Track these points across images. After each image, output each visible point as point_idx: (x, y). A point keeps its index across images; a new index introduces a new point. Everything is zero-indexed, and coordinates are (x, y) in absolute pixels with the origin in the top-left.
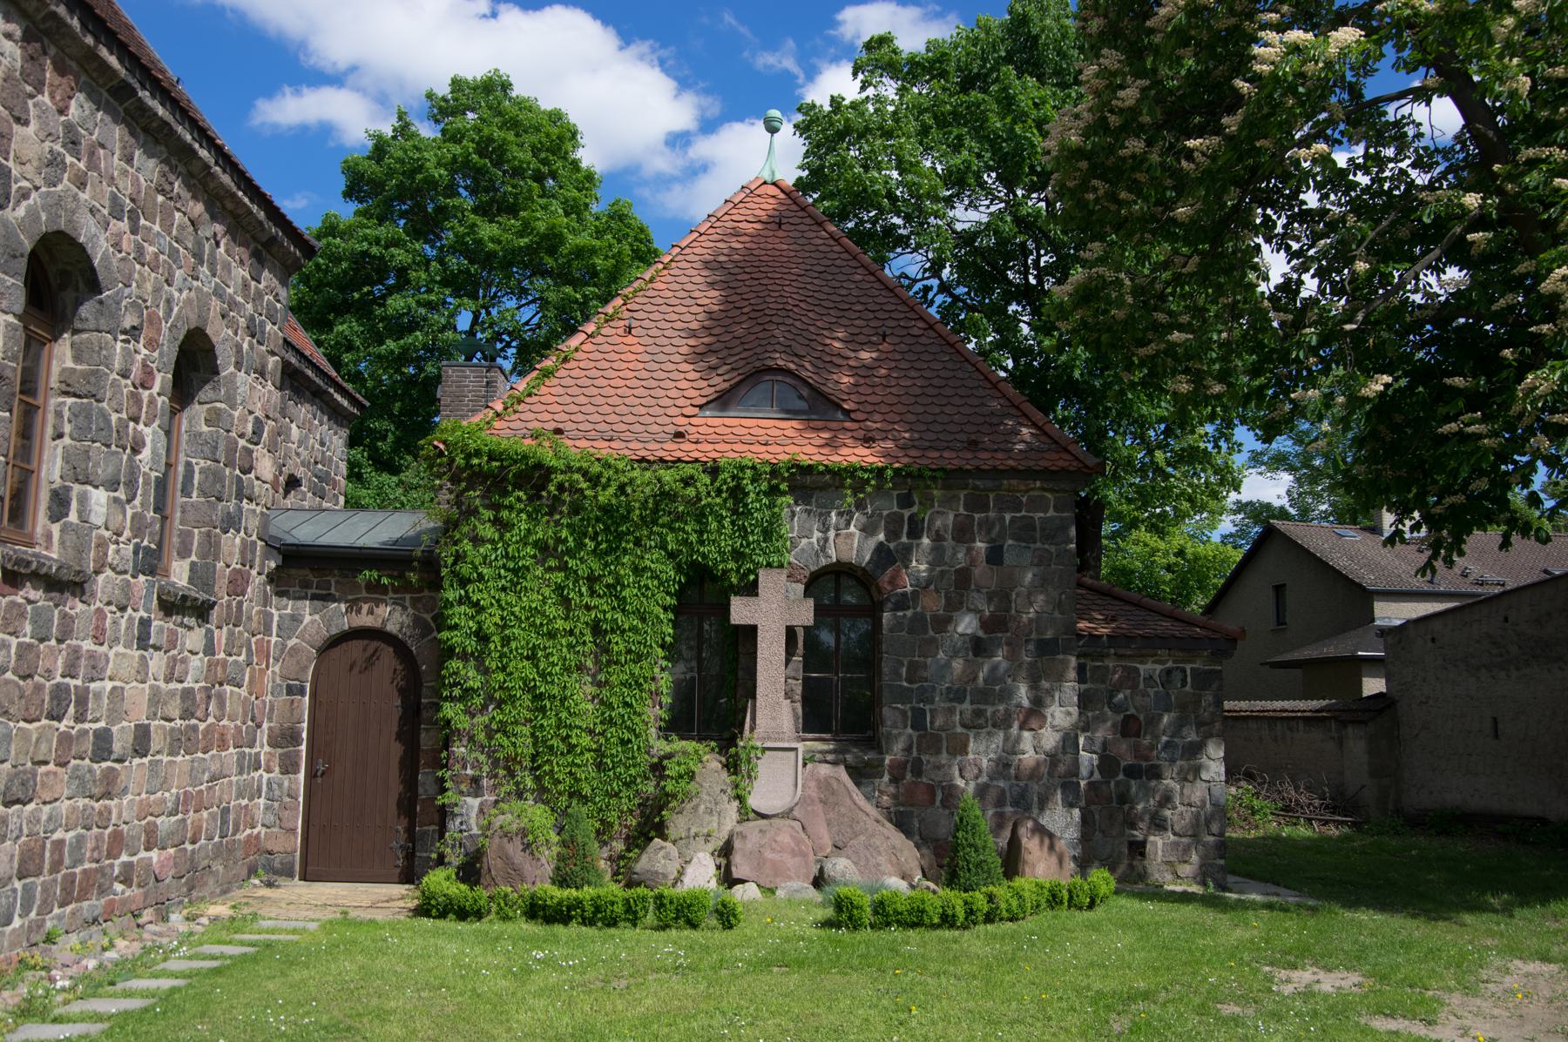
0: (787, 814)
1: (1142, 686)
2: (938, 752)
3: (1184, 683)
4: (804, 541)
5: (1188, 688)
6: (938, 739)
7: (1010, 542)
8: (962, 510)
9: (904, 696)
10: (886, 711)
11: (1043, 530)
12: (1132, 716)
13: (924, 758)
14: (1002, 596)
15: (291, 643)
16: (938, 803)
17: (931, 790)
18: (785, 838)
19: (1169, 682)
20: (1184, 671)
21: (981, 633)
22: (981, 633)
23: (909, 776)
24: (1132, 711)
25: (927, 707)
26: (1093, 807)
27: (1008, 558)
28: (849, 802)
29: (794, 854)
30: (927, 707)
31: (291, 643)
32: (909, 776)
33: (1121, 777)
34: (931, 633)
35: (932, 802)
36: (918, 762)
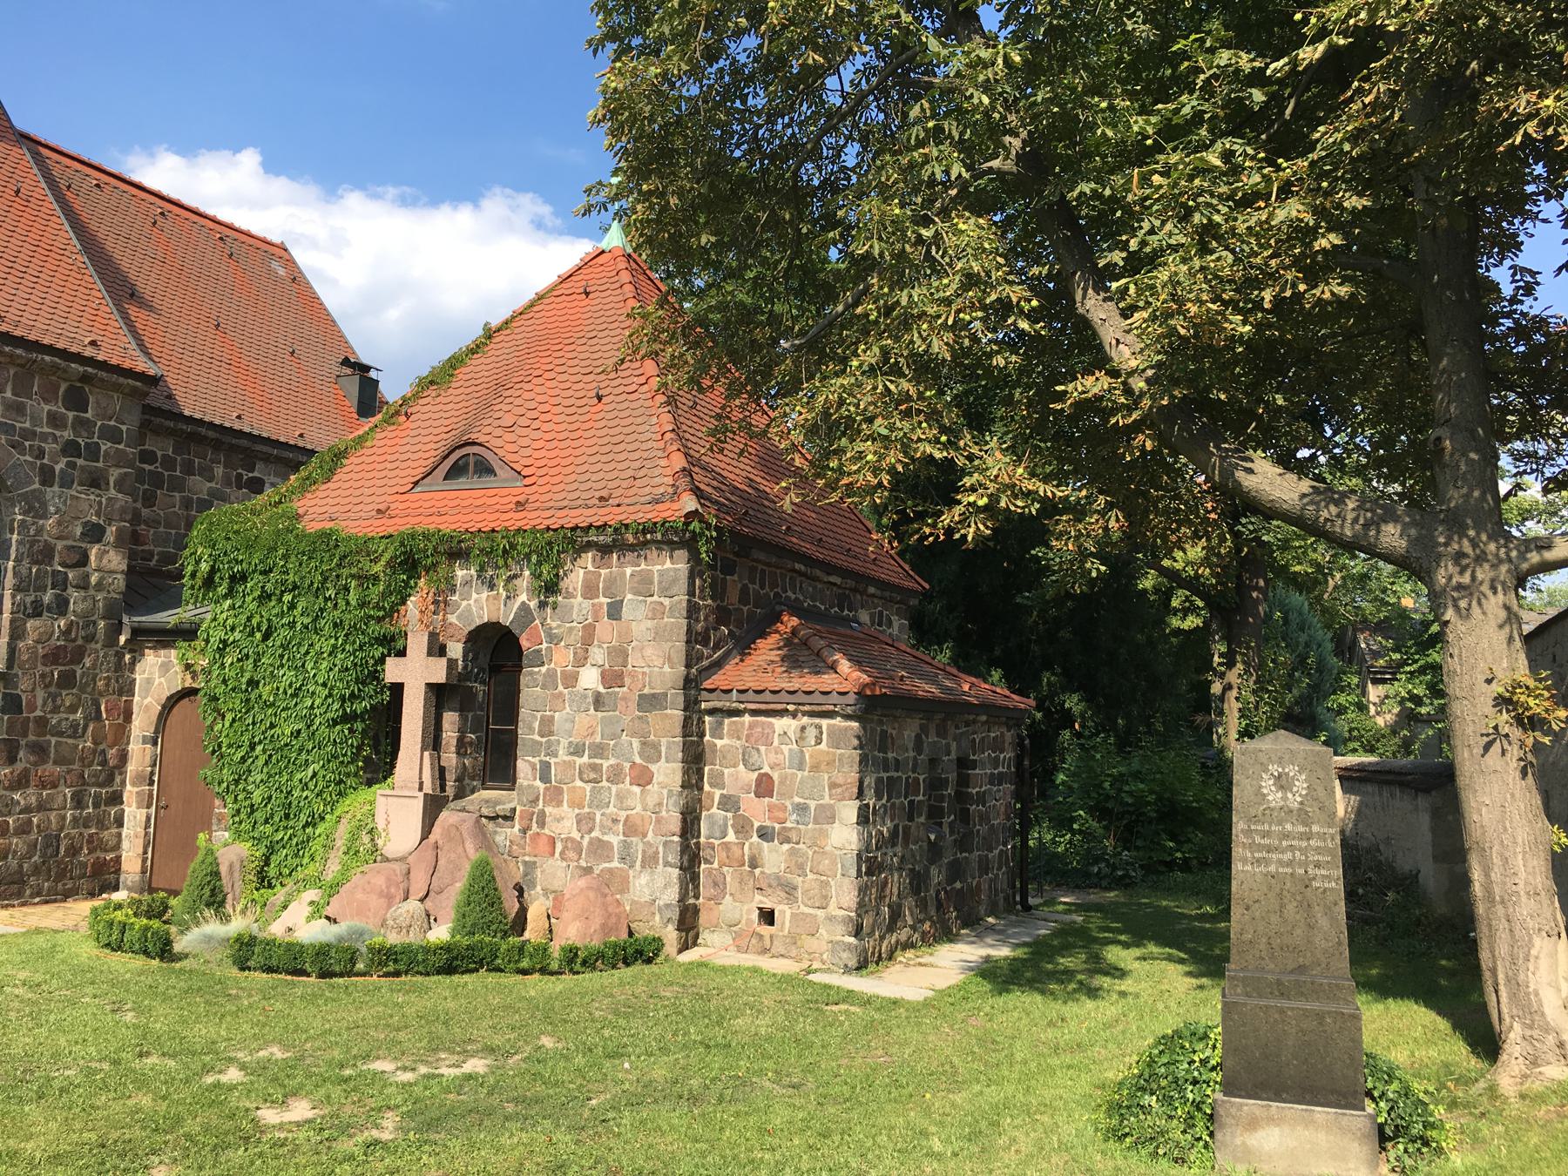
0: (402, 859)
1: (776, 743)
2: (559, 804)
3: (819, 741)
4: (464, 603)
5: (823, 746)
6: (559, 791)
7: (629, 596)
8: (590, 567)
9: (535, 749)
10: (520, 763)
11: (660, 582)
12: (766, 775)
13: (548, 810)
14: (620, 653)
15: (146, 702)
16: (557, 855)
17: (552, 841)
18: (380, 881)
19: (802, 738)
20: (819, 727)
21: (601, 689)
22: (601, 689)
23: (534, 825)
24: (766, 769)
25: (553, 761)
26: (725, 869)
27: (626, 612)
28: (460, 849)
29: (381, 894)
30: (553, 761)
31: (146, 702)
32: (534, 825)
33: (755, 838)
34: (560, 688)
35: (553, 854)
36: (542, 814)
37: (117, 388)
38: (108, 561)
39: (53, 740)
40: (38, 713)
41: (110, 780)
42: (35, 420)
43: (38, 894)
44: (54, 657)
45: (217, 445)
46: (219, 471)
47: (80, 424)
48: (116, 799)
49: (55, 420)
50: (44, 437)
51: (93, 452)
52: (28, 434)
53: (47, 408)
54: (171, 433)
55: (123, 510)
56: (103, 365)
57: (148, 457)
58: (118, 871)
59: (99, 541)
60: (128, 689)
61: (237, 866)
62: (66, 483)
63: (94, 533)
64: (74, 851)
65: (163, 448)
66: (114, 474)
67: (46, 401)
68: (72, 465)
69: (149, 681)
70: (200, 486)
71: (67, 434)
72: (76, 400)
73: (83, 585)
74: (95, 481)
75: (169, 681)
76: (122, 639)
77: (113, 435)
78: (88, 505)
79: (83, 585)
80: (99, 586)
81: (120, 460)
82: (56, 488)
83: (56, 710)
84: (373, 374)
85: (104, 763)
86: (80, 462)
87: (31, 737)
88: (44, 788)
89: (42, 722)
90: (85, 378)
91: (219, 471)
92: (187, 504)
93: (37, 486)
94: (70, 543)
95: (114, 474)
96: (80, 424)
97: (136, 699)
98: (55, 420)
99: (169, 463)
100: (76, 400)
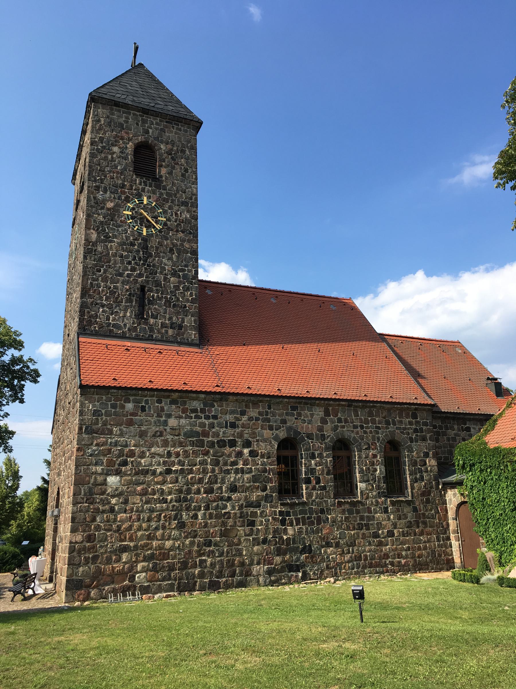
37: (424, 410)
38: (432, 463)
39: (428, 520)
40: (422, 512)
41: (445, 533)
42: (406, 425)
43: (433, 569)
44: (423, 494)
45: (454, 419)
46: (456, 427)
47: (417, 423)
48: (448, 538)
49: (410, 423)
50: (408, 429)
51: (421, 430)
52: (405, 429)
53: (407, 420)
54: (440, 418)
55: (433, 446)
56: (420, 404)
57: (435, 427)
58: (454, 562)
59: (428, 457)
60: (445, 502)
61: (492, 559)
62: (416, 442)
63: (426, 455)
64: (440, 555)
65: (438, 423)
66: (428, 436)
67: (407, 418)
68: (417, 435)
69: (451, 500)
70: (451, 433)
71: (414, 427)
72: (415, 416)
73: (427, 471)
74: (424, 439)
75: (457, 499)
76: (440, 487)
77: (426, 424)
78: (423, 446)
79: (427, 471)
80: (431, 471)
81: (429, 431)
82: (414, 443)
83: (426, 511)
84: (499, 381)
85: (443, 527)
86: (419, 434)
87: (422, 519)
88: (428, 535)
89: (424, 514)
90: (416, 409)
91: (456, 427)
92: (448, 439)
93: (409, 443)
94: (421, 459)
95: (428, 436)
96: (417, 423)
97: (448, 506)
98: (410, 423)
99: (441, 427)
100: (415, 416)
